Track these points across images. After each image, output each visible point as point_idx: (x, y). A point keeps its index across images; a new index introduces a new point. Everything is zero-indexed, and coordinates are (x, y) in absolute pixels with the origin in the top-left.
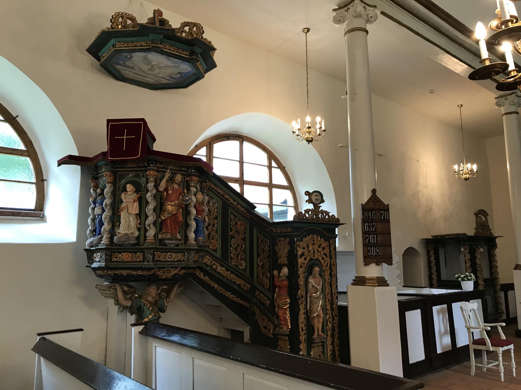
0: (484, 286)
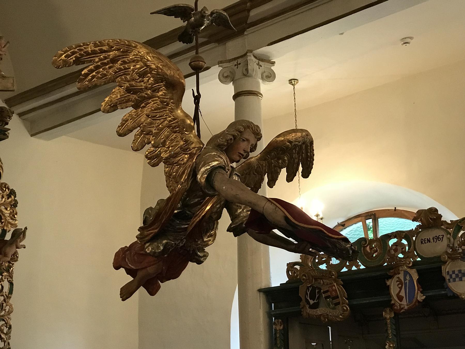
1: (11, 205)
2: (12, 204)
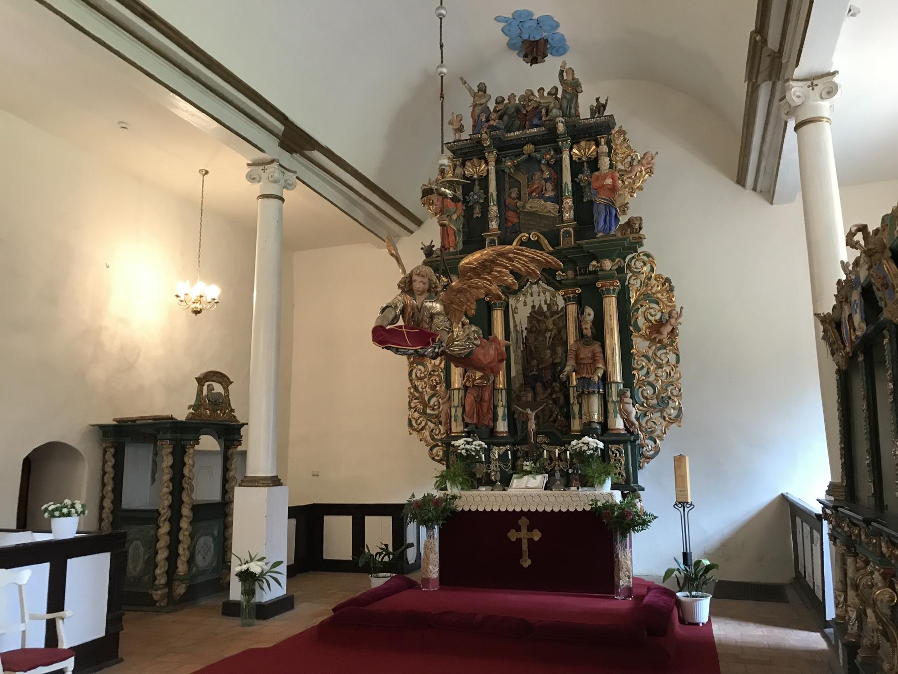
0: (191, 519)
1: (667, 291)
2: (668, 290)
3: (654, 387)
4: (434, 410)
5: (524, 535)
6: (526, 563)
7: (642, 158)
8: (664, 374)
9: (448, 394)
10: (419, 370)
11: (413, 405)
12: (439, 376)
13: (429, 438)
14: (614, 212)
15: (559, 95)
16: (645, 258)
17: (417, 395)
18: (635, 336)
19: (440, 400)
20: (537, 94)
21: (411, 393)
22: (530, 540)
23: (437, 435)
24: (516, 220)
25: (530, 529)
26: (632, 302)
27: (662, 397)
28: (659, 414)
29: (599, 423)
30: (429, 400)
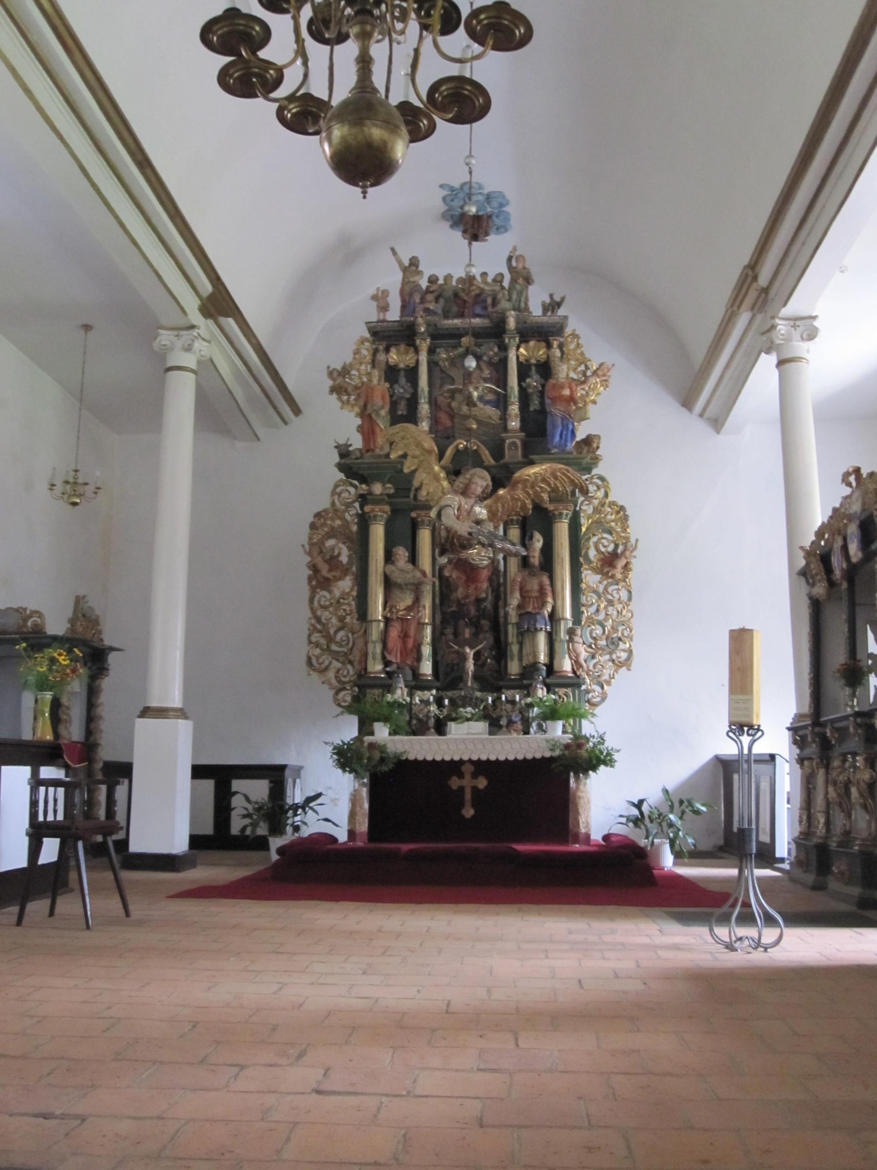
3: (603, 627)
4: (341, 646)
5: (467, 783)
6: (469, 812)
7: (598, 369)
8: (615, 613)
9: (363, 629)
10: (323, 595)
11: (313, 639)
12: (349, 604)
13: (334, 681)
14: (570, 427)
15: (506, 283)
16: (599, 482)
17: (319, 627)
18: (586, 569)
19: (350, 635)
20: (479, 278)
21: (312, 625)
22: (475, 789)
23: (345, 676)
24: (448, 423)
25: (475, 776)
26: (584, 529)
27: (612, 638)
28: (608, 657)
29: (545, 665)
30: (336, 633)
